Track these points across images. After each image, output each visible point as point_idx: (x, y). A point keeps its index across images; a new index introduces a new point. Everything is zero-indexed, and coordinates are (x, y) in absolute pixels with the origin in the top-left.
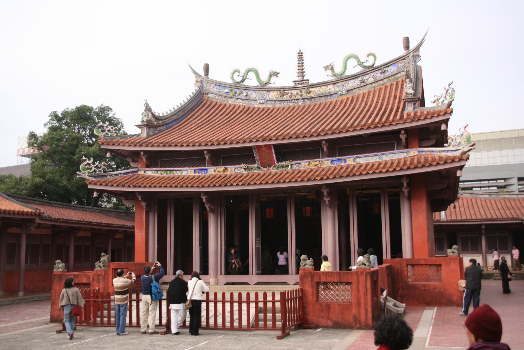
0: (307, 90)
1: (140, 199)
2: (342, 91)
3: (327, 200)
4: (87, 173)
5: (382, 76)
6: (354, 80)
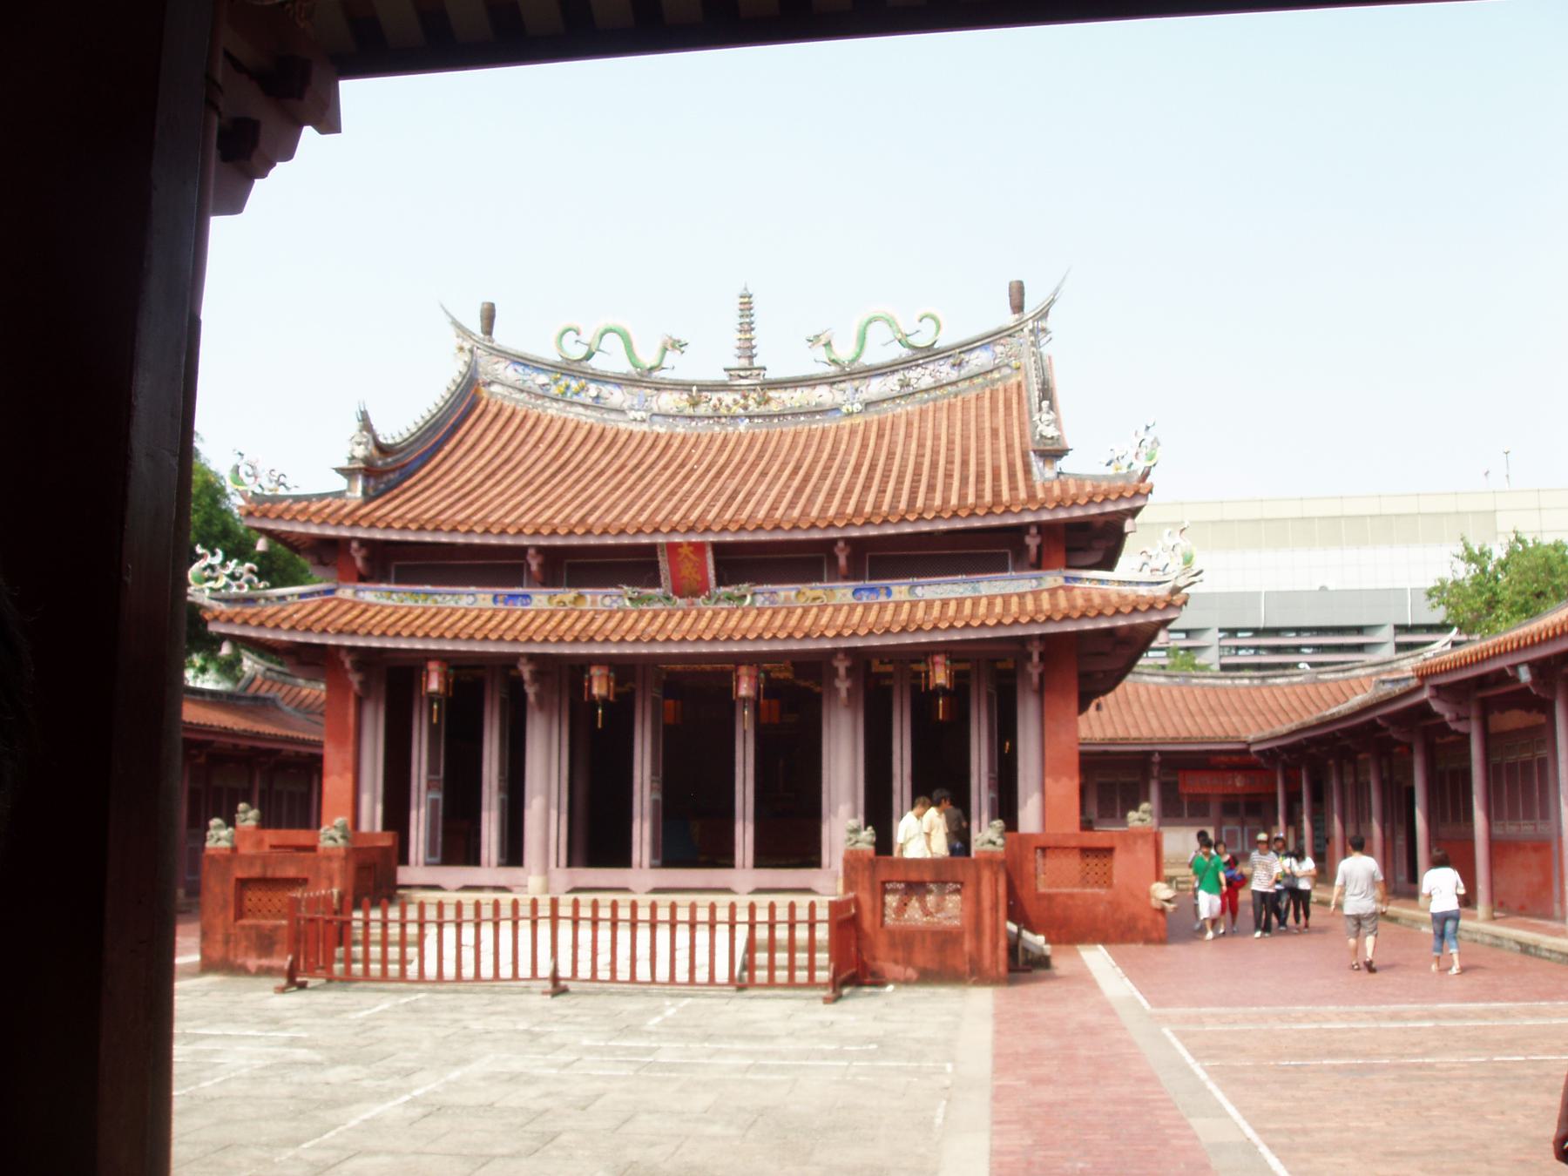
0: (761, 393)
1: (348, 665)
2: (852, 404)
3: (843, 686)
4: (207, 592)
5: (954, 375)
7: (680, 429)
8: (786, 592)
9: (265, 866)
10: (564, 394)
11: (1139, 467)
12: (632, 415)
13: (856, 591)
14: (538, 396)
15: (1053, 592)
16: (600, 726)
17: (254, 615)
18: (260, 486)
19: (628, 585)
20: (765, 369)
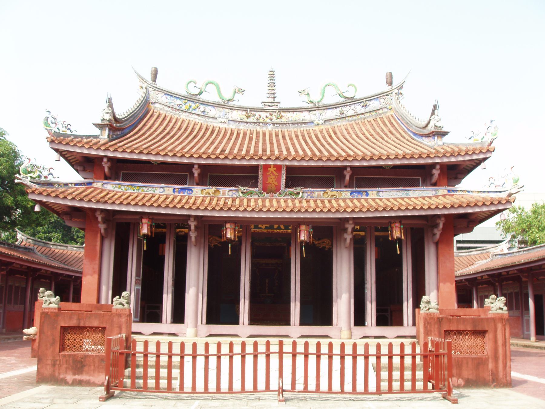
0: (279, 114)
1: (100, 219)
2: (319, 120)
3: (348, 237)
4: (29, 178)
5: (363, 110)
6: (333, 109)
7: (242, 127)
8: (318, 192)
9: (79, 319)
10: (188, 109)
11: (487, 140)
12: (219, 120)
13: (352, 193)
14: (176, 110)
15: (444, 196)
16: (230, 253)
17: (53, 192)
18: (58, 128)
19: (242, 186)
20: (280, 103)
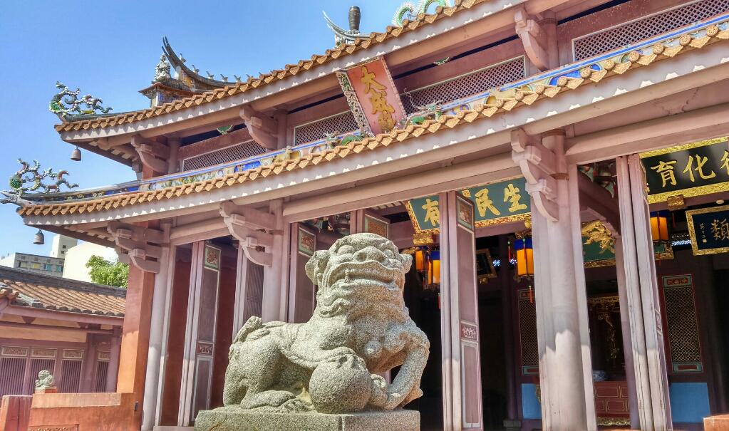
8: (475, 103)
